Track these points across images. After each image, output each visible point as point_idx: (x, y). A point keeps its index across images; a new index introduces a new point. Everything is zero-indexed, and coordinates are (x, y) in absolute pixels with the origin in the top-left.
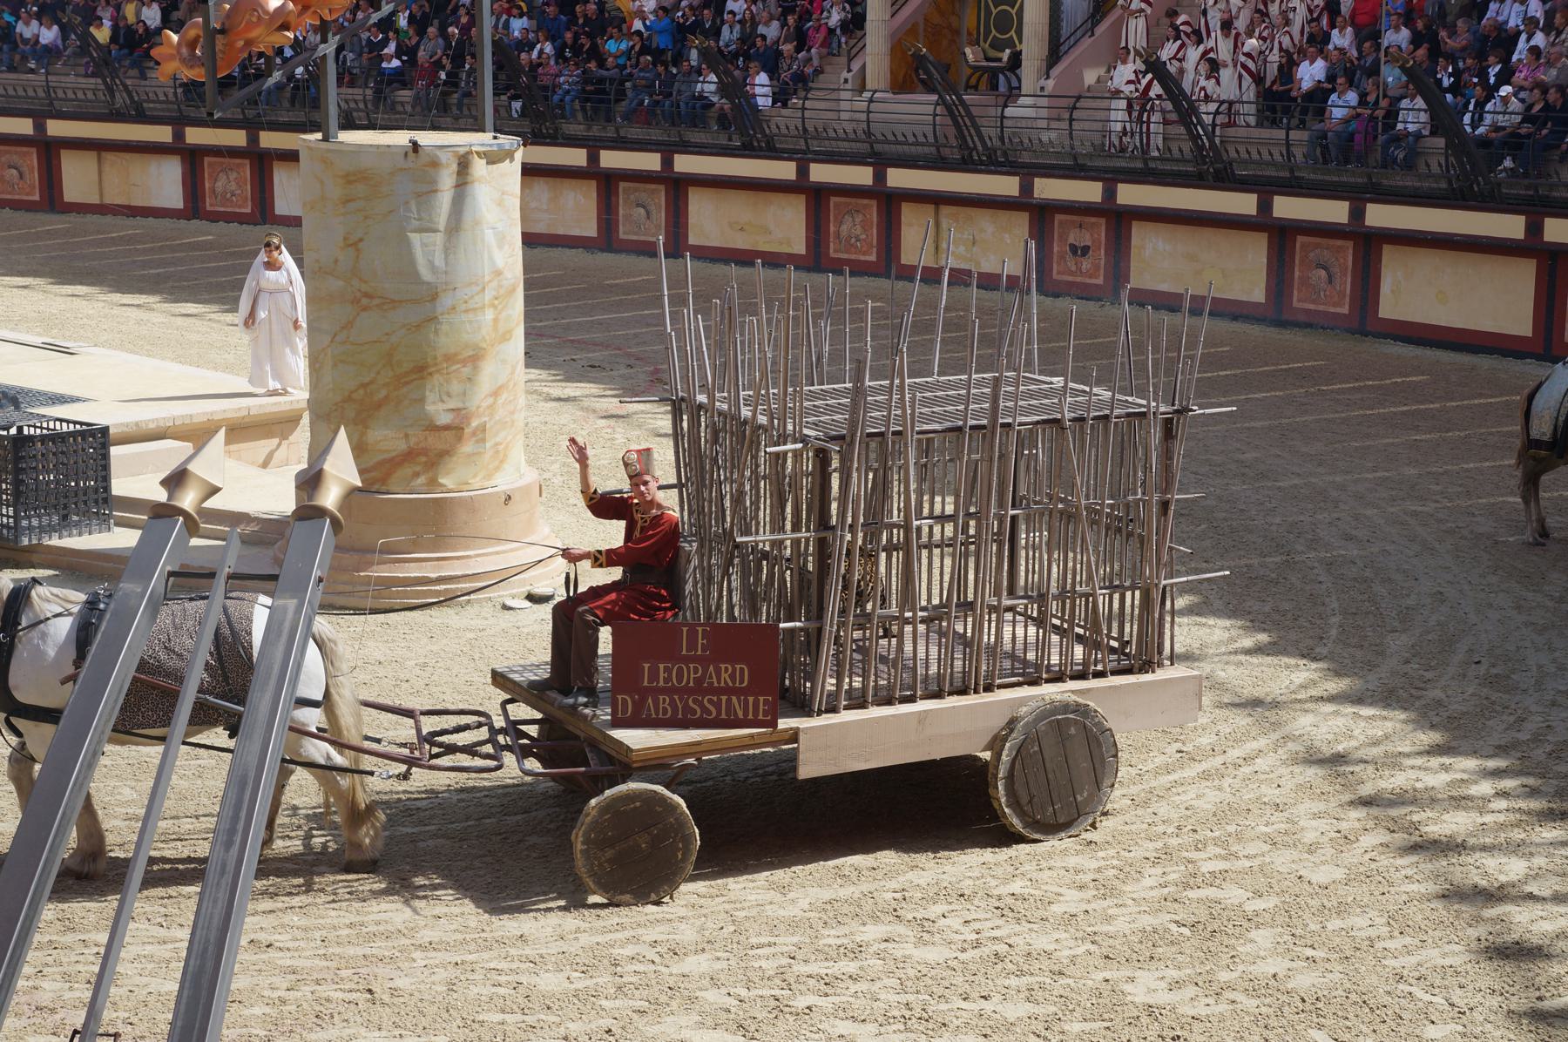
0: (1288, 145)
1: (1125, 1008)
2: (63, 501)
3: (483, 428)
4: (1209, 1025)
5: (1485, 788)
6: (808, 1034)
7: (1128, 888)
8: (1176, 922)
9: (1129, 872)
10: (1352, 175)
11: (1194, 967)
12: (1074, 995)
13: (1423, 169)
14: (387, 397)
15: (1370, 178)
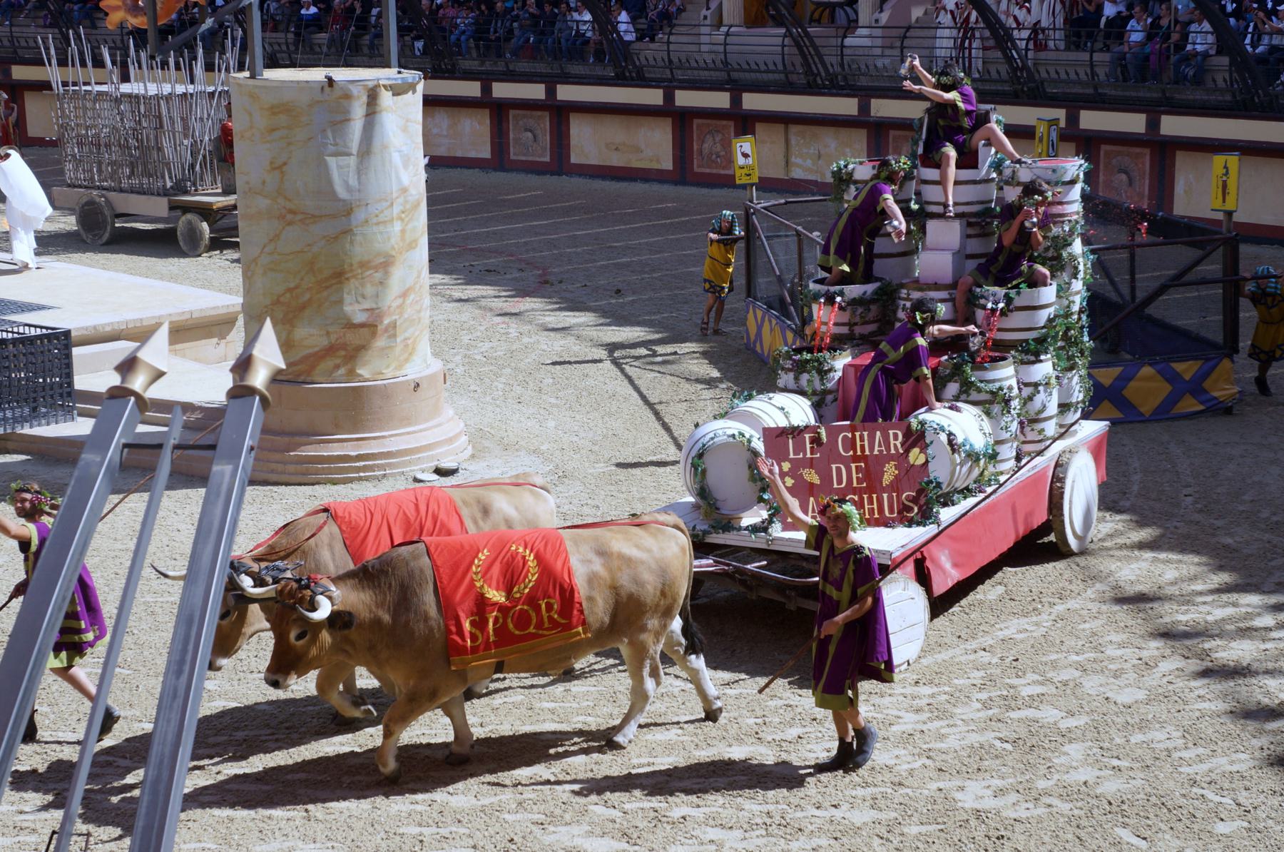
0: (1092, 66)
1: (957, 813)
2: (33, 395)
3: (394, 325)
4: (1029, 826)
5: (1268, 620)
6: (683, 840)
7: (958, 711)
8: (1000, 739)
9: (959, 696)
10: (1149, 91)
11: (1016, 776)
12: (912, 803)
13: (1210, 84)
14: (310, 300)
15: (1163, 92)
